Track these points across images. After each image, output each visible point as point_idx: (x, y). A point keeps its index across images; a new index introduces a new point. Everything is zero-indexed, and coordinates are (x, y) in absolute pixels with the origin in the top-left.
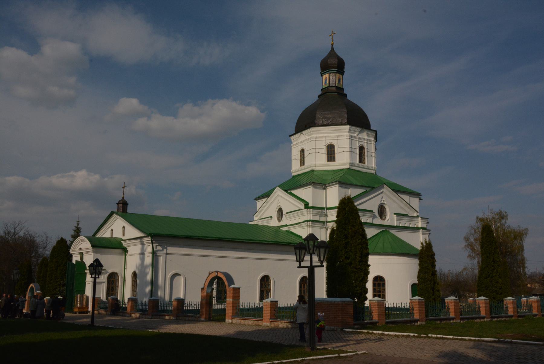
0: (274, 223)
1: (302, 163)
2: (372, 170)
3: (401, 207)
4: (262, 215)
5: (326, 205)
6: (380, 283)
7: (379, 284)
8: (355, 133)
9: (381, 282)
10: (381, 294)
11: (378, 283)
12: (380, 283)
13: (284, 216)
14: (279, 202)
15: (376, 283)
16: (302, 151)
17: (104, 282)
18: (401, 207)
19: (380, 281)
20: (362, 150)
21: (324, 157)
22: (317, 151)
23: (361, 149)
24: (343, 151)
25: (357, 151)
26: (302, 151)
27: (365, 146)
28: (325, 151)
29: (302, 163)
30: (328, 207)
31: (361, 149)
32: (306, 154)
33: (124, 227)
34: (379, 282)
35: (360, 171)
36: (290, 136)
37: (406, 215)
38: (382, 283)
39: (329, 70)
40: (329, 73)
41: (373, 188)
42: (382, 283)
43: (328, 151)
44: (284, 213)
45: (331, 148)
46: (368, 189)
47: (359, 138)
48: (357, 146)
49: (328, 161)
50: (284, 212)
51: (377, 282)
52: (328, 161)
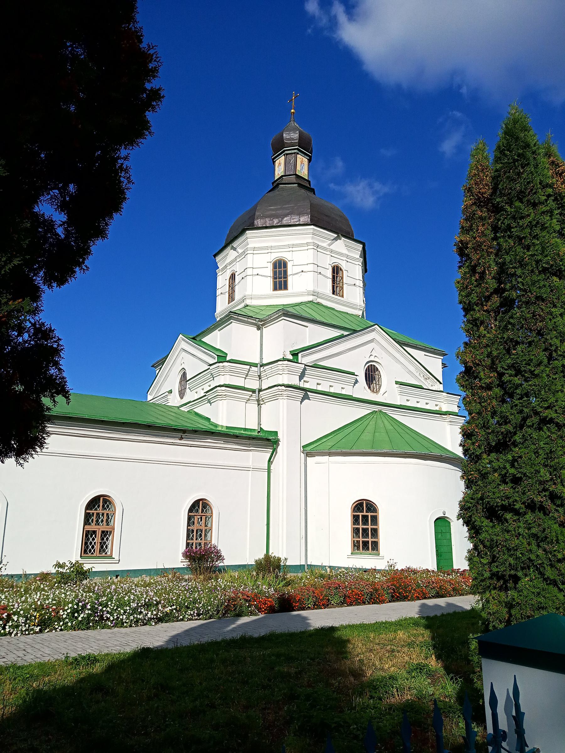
0: (174, 400)
2: (356, 309)
3: (410, 372)
5: (261, 358)
6: (368, 516)
7: (365, 518)
8: (324, 242)
9: (369, 514)
10: (370, 540)
11: (362, 515)
12: (368, 516)
14: (182, 362)
15: (359, 515)
18: (410, 372)
19: (367, 512)
21: (269, 283)
22: (256, 271)
23: (336, 270)
24: (302, 271)
25: (329, 274)
27: (343, 265)
28: (269, 271)
30: (265, 362)
31: (336, 270)
34: (365, 513)
35: (333, 309)
36: (215, 256)
38: (371, 516)
39: (285, 149)
40: (284, 155)
41: (355, 331)
42: (371, 516)
43: (275, 273)
45: (280, 267)
47: (332, 251)
48: (327, 262)
49: (275, 289)
51: (361, 514)
52: (275, 289)
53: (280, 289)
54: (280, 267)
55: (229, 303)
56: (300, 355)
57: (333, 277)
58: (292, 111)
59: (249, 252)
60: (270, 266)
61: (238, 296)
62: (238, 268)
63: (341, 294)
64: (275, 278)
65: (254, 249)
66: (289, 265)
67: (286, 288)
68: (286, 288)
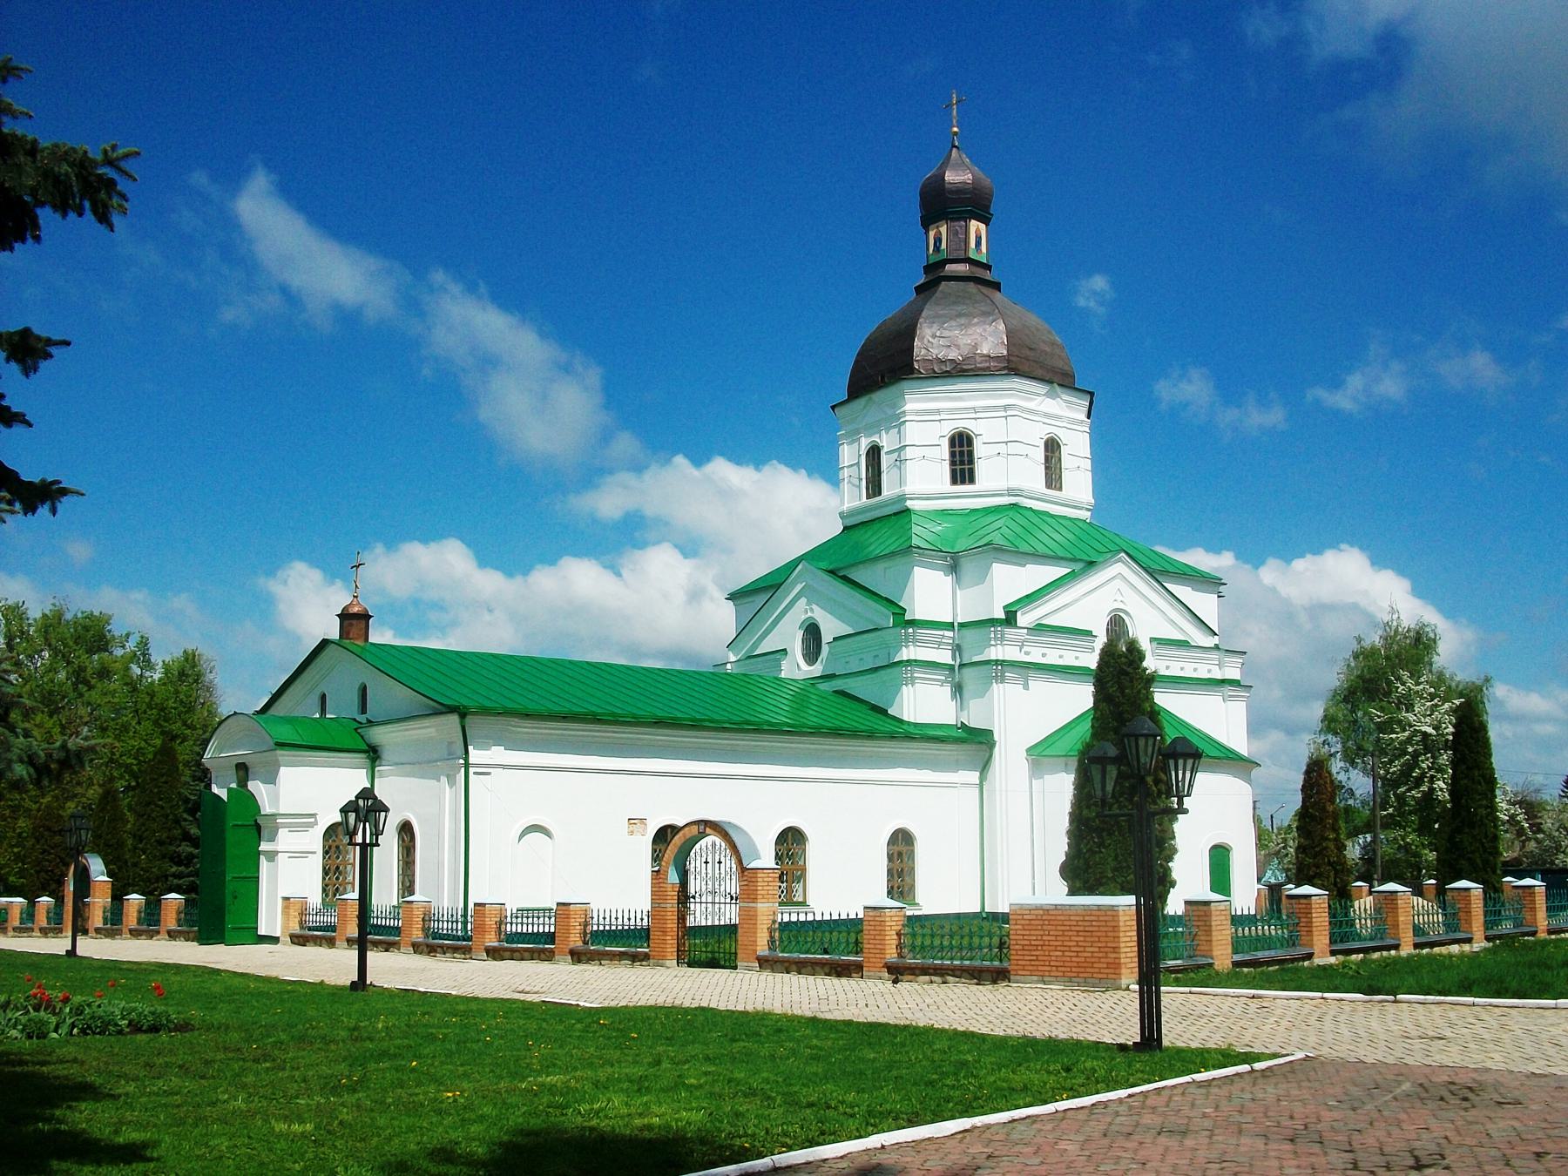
1: (874, 486)
2: (1081, 509)
4: (756, 645)
13: (825, 649)
16: (874, 453)
17: (315, 853)
20: (1053, 452)
26: (874, 453)
27: (1064, 436)
29: (874, 486)
32: (885, 461)
33: (363, 691)
35: (1046, 513)
37: (1183, 644)
41: (1091, 564)
43: (953, 454)
44: (823, 641)
46: (1078, 566)
49: (954, 481)
50: (827, 637)
52: (954, 481)
53: (963, 482)
55: (868, 497)
56: (1019, 614)
57: (1047, 458)
58: (955, 129)
59: (907, 418)
60: (945, 443)
61: (888, 491)
62: (886, 441)
63: (1058, 486)
64: (953, 463)
65: (918, 412)
66: (977, 444)
67: (972, 481)
68: (972, 481)
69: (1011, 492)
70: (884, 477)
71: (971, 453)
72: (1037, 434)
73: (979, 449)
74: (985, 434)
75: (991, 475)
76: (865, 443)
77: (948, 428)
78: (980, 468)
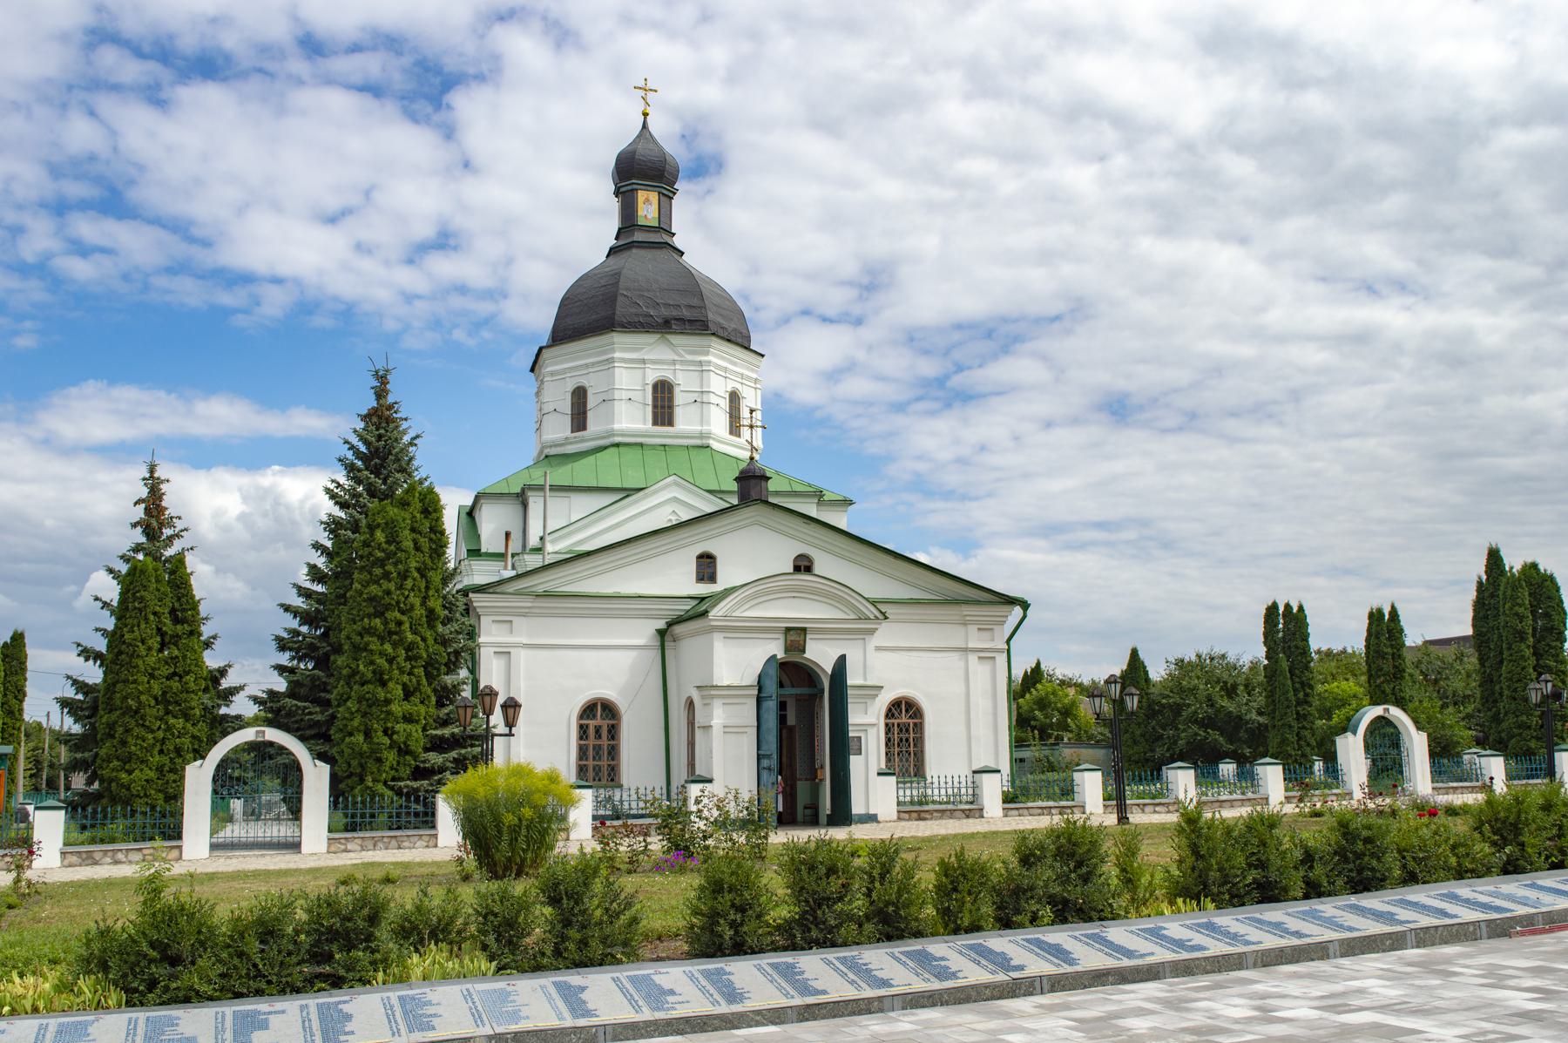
1: (579, 419)
16: (580, 395)
25: (725, 404)
26: (580, 395)
29: (579, 419)
32: (591, 401)
43: (655, 399)
45: (663, 392)
49: (655, 423)
53: (663, 424)
54: (663, 392)
55: (572, 432)
61: (594, 425)
64: (655, 406)
67: (671, 423)
68: (671, 423)
69: (702, 436)
70: (590, 414)
71: (671, 399)
72: (719, 387)
73: (679, 398)
74: (684, 384)
75: (685, 422)
76: (570, 386)
77: (653, 376)
78: (680, 414)
